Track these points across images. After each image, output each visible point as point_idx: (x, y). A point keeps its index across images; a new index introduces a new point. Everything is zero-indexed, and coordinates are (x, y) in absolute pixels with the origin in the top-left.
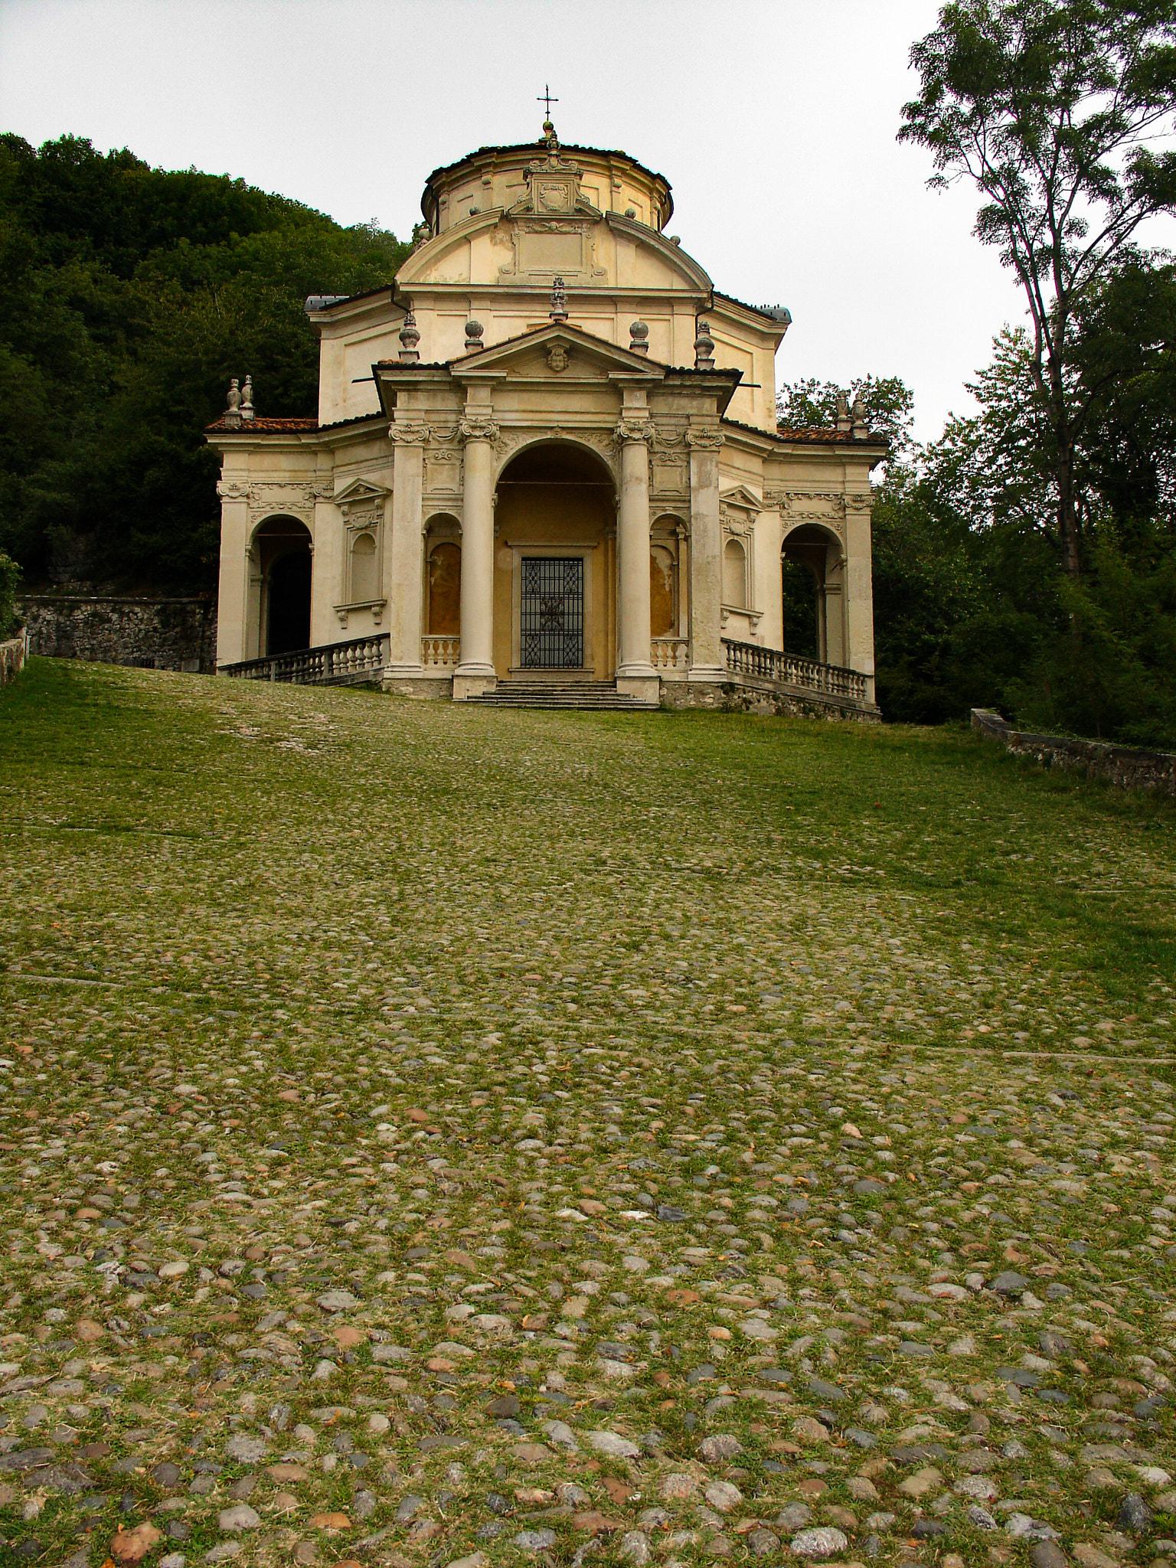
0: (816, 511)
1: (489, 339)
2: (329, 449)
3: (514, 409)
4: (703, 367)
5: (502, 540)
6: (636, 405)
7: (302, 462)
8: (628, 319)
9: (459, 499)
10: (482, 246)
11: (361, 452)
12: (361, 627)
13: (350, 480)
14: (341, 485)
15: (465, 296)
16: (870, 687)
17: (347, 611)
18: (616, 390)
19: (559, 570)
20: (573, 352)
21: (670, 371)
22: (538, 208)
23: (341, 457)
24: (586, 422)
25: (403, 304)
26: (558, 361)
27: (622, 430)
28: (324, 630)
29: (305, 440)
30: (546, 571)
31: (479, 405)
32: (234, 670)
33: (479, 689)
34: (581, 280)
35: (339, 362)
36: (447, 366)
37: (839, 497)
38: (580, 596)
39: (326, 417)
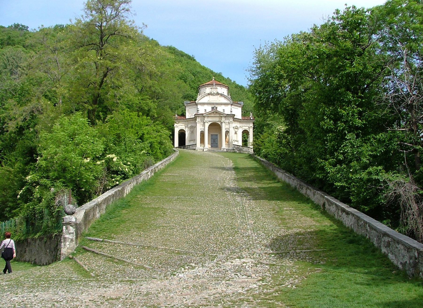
0: (246, 128)
1: (207, 111)
2: (187, 121)
3: (210, 119)
4: (231, 114)
5: (208, 133)
6: (223, 119)
7: (184, 122)
8: (223, 107)
9: (204, 129)
10: (206, 97)
11: (192, 122)
12: (192, 143)
13: (190, 125)
14: (189, 126)
15: (203, 104)
16: (252, 150)
17: (190, 141)
18: (221, 117)
19: (215, 136)
20: (216, 112)
21: (227, 115)
22: (212, 93)
23: (189, 122)
24: (218, 120)
25: (197, 105)
26: (215, 113)
27: (222, 121)
28: (187, 144)
29: (185, 120)
30: (214, 136)
31: (206, 119)
32: (176, 147)
33: (207, 150)
34: (218, 102)
35: (188, 110)
36: (202, 114)
37: (249, 126)
38: (217, 139)
39: (187, 118)
